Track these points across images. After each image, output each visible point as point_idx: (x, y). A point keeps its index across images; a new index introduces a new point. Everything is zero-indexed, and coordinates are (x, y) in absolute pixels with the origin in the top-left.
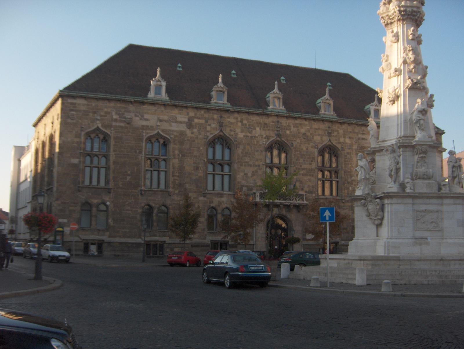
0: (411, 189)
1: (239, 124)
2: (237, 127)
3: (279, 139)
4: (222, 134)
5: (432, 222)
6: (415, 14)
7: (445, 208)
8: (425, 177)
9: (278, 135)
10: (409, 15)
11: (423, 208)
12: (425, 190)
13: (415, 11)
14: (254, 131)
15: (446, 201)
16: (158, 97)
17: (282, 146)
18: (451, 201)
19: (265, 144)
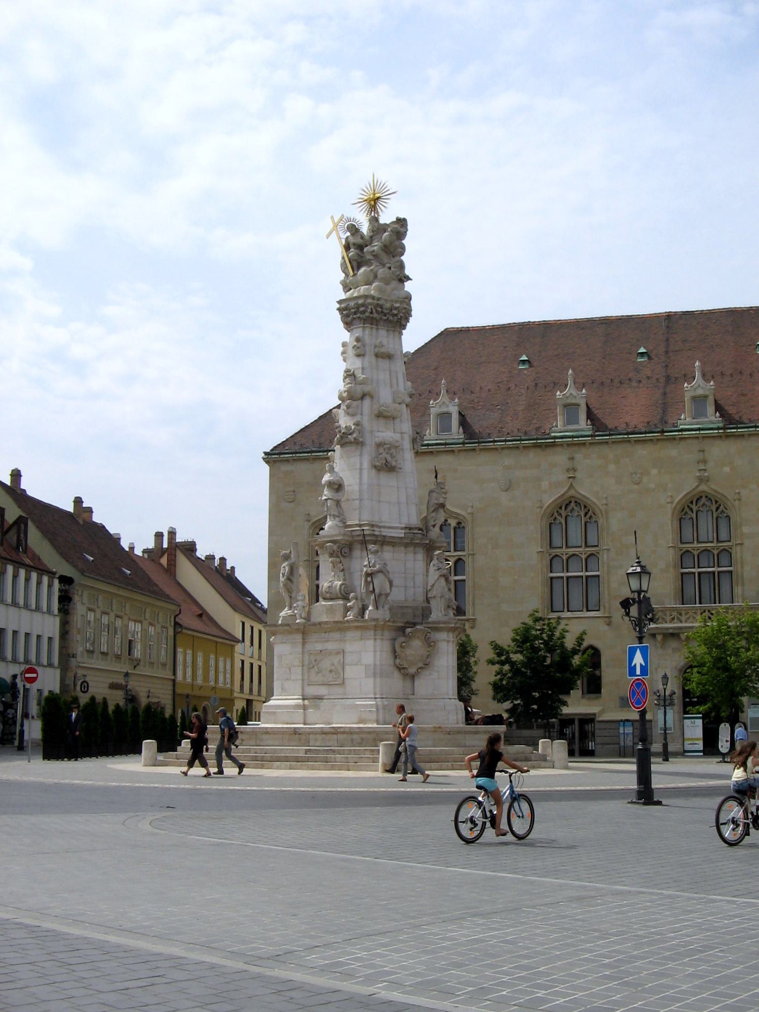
0: (301, 617)
1: (612, 467)
2: (601, 476)
3: (703, 487)
4: (572, 493)
5: (331, 671)
6: (362, 309)
7: (348, 647)
8: (328, 595)
9: (701, 480)
10: (355, 313)
11: (319, 647)
12: (325, 619)
13: (363, 305)
14: (645, 479)
15: (350, 635)
16: (445, 437)
17: (716, 502)
18: (358, 633)
19: (672, 503)
